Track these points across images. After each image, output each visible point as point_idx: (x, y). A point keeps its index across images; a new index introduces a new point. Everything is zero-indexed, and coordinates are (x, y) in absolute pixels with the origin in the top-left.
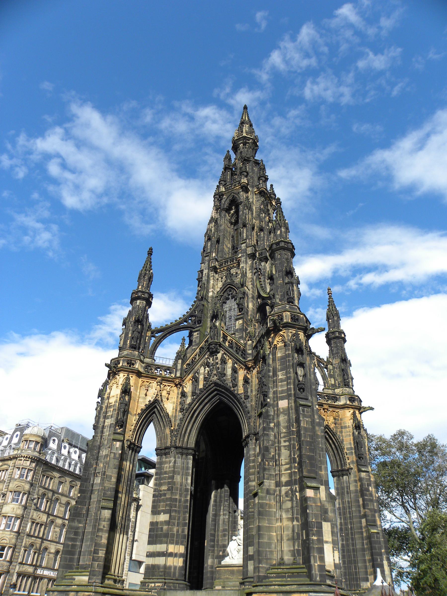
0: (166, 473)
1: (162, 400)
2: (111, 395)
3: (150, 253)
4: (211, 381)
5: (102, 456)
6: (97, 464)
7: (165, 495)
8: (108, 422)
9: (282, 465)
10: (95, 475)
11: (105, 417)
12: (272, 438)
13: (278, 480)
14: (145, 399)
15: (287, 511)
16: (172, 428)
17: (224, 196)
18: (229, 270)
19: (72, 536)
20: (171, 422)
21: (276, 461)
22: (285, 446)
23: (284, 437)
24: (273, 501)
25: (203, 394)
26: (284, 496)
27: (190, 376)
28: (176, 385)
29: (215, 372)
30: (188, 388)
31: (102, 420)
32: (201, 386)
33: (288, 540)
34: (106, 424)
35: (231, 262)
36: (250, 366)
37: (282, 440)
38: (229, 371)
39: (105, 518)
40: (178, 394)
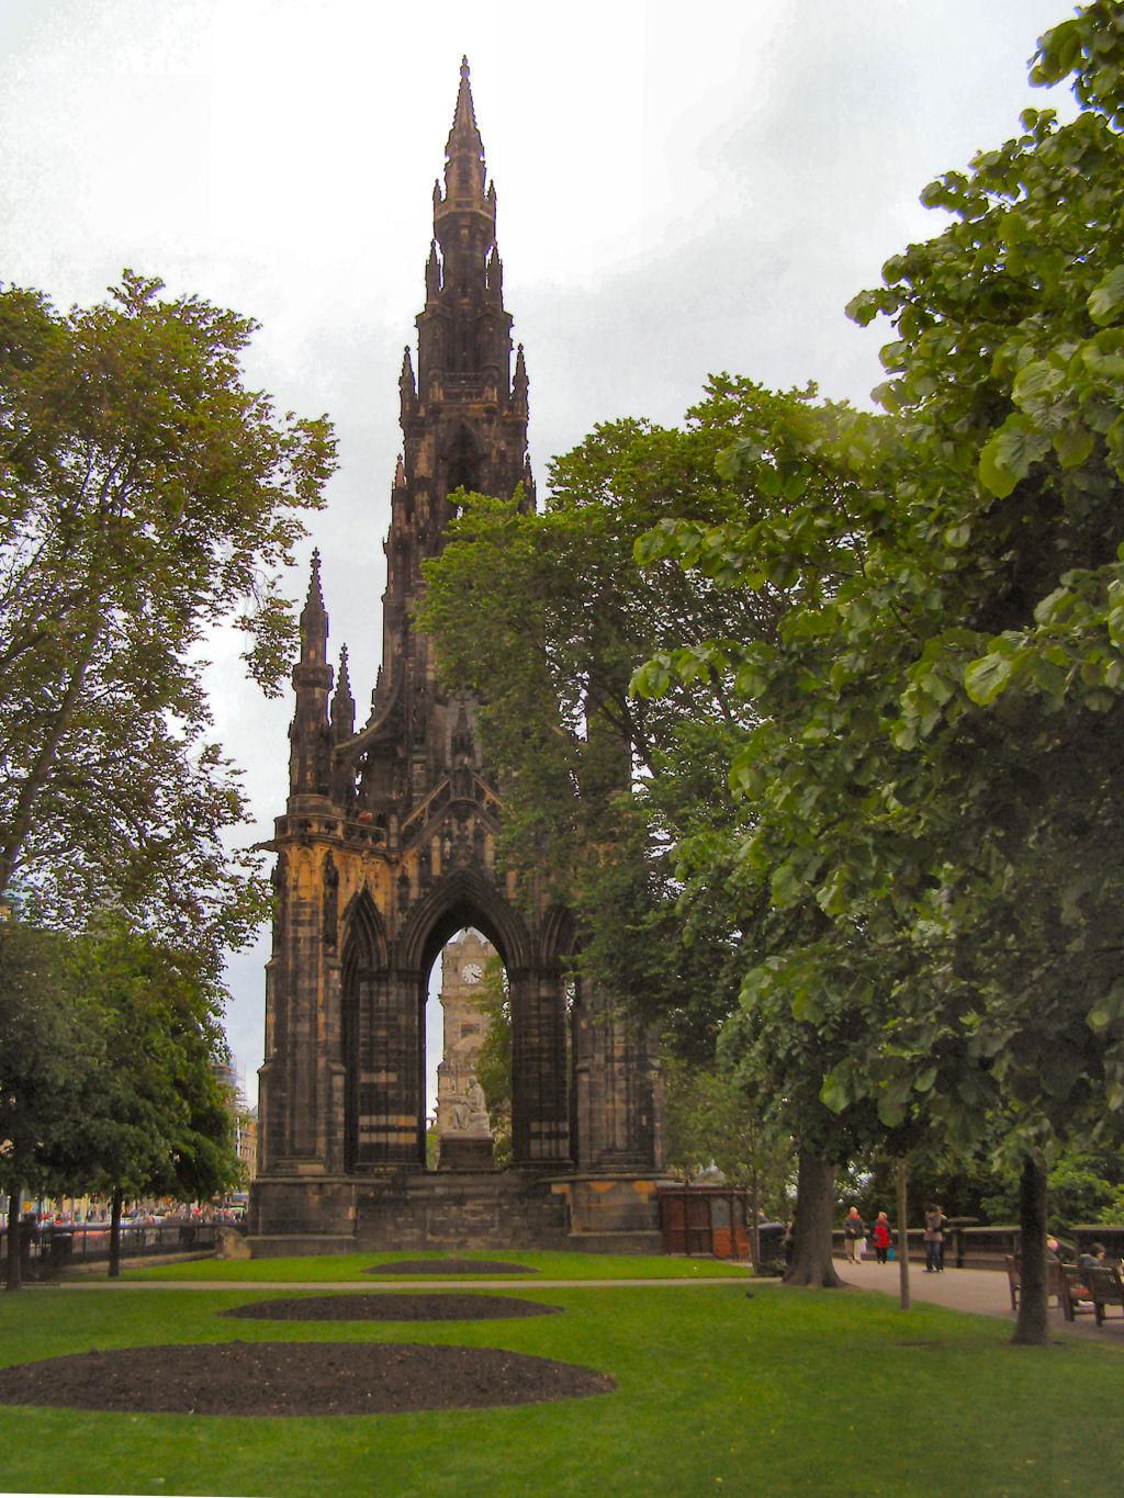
0: (381, 1010)
2: (300, 884)
6: (296, 1001)
7: (386, 1044)
8: (304, 932)
10: (296, 1020)
11: (297, 923)
14: (347, 887)
15: (620, 1092)
16: (389, 939)
17: (442, 416)
19: (276, 1110)
21: (607, 1030)
27: (415, 849)
28: (389, 861)
29: (462, 852)
30: (412, 870)
31: (290, 927)
33: (622, 1124)
34: (300, 935)
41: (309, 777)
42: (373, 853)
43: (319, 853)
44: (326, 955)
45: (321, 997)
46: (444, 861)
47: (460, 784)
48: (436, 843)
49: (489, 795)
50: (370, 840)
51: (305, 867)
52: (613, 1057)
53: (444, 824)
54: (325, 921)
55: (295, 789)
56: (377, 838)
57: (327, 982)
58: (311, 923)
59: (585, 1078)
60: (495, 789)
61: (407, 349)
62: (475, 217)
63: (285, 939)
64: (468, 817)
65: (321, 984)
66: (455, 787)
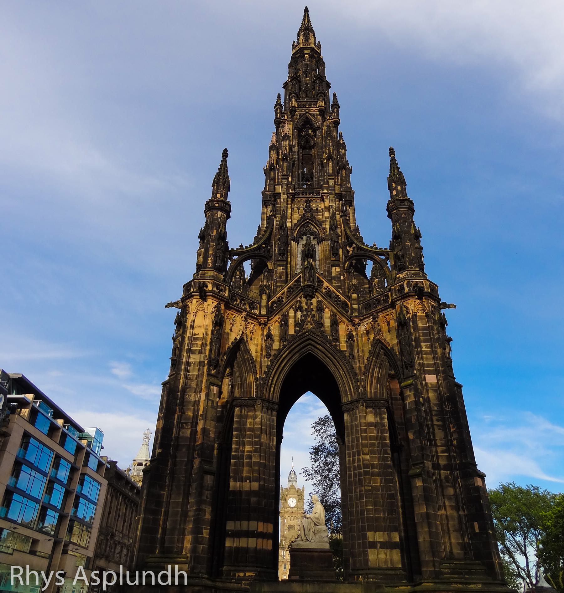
1: (247, 340)
2: (196, 324)
3: (225, 154)
4: (305, 329)
5: (190, 402)
6: (183, 412)
8: (195, 358)
9: (438, 446)
10: (181, 425)
11: (190, 351)
12: (423, 414)
13: (436, 461)
15: (450, 498)
18: (308, 202)
20: (255, 367)
21: (430, 441)
22: (438, 426)
23: (436, 415)
24: (433, 485)
25: (295, 341)
26: (444, 481)
27: (277, 317)
29: (309, 319)
30: (275, 329)
31: (185, 354)
32: (291, 331)
34: (191, 360)
35: (310, 194)
36: (356, 322)
37: (435, 418)
38: (327, 322)
39: (208, 486)
40: (262, 335)
41: (209, 261)
42: (250, 316)
43: (211, 304)
44: (209, 375)
45: (201, 408)
46: (297, 324)
47: (308, 275)
48: (291, 313)
49: (326, 284)
50: (247, 306)
51: (200, 314)
52: (438, 464)
53: (297, 301)
54: (211, 350)
55: (200, 267)
56: (252, 307)
57: (207, 395)
58: (200, 352)
59: (419, 483)
60: (330, 281)
61: (279, 95)
62: (312, 49)
63: (180, 363)
64: (312, 297)
65: (203, 395)
66: (304, 278)
